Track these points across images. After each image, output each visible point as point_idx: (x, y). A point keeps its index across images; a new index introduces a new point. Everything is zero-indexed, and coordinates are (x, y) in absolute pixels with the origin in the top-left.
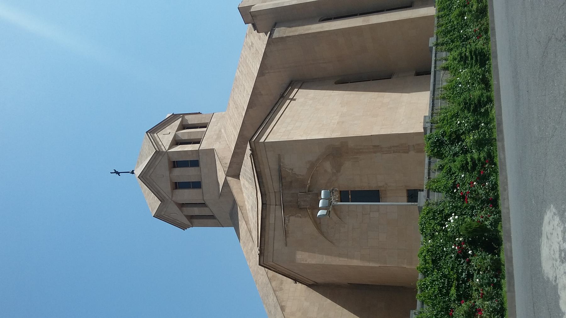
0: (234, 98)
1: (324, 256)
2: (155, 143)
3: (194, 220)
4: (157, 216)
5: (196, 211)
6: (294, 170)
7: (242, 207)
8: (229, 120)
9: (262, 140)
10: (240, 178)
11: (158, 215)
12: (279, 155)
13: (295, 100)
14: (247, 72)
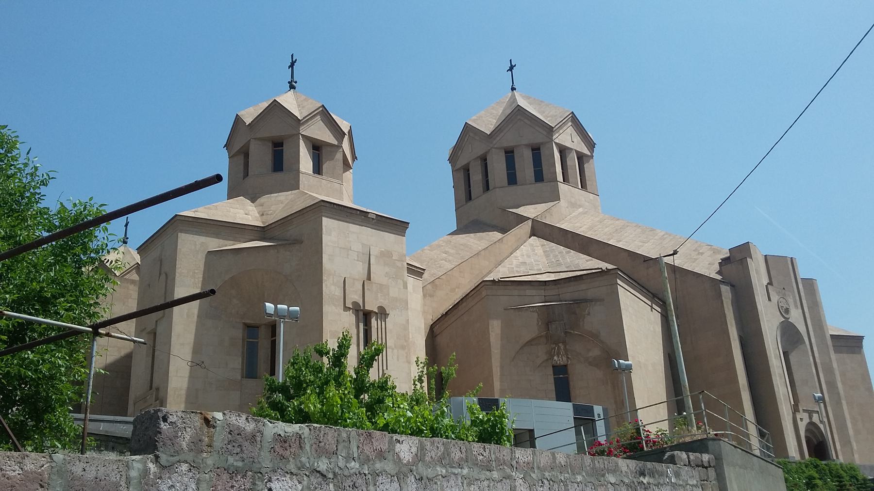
2: (562, 125)
5: (476, 177)
6: (588, 316)
7: (502, 242)
8: (598, 219)
9: (619, 282)
10: (532, 237)
11: (468, 128)
12: (603, 300)
13: (652, 311)
14: (665, 246)
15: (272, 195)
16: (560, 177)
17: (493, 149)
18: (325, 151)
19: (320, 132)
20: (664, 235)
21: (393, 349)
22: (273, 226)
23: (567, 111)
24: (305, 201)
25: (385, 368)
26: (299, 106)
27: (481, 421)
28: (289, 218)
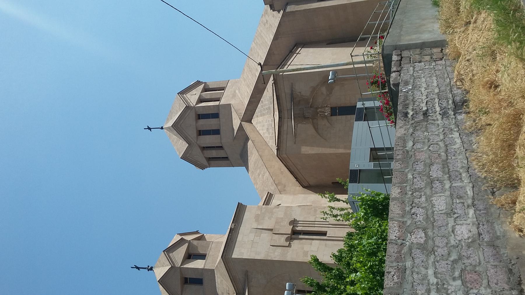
0: (248, 64)
1: (320, 148)
2: (185, 101)
3: (211, 161)
4: (183, 157)
5: (214, 153)
10: (252, 122)
11: (184, 157)
12: (292, 83)
13: (300, 54)
14: (261, 42)
15: (217, 287)
16: (217, 103)
17: (197, 143)
18: (191, 252)
19: (180, 254)
20: (255, 43)
21: (316, 217)
22: (236, 288)
23: (177, 96)
24: (221, 267)
25: (328, 223)
26: (163, 266)
27: (365, 214)
28: (231, 277)
